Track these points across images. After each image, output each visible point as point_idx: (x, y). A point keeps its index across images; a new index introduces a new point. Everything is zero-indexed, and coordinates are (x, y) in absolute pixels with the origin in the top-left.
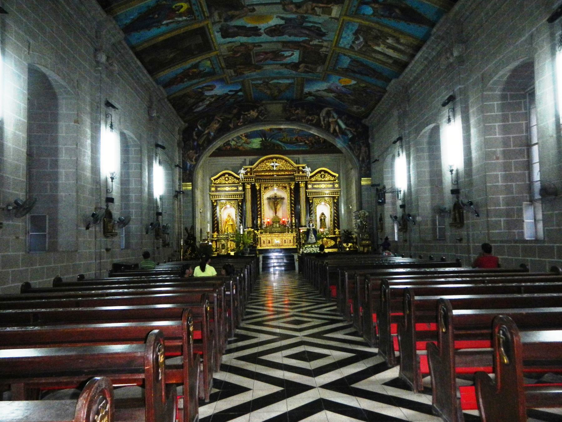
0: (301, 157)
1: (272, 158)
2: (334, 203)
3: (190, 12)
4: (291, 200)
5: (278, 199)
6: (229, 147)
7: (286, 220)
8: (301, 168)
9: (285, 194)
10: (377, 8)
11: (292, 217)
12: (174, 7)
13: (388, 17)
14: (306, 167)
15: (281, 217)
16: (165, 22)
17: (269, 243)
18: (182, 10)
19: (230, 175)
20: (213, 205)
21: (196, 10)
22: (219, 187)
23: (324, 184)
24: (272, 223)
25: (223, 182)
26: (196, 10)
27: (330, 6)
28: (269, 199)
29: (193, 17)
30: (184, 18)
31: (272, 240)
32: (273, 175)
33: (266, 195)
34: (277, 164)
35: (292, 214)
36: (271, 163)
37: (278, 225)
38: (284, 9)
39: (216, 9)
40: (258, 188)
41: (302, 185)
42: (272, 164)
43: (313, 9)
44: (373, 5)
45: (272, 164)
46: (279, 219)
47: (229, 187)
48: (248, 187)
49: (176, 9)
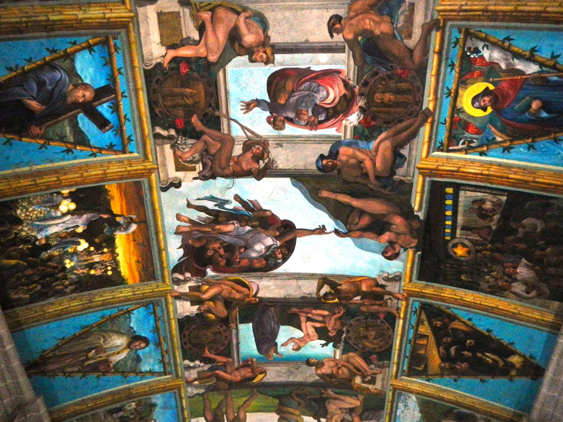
3: (468, 69)
10: (76, 86)
12: (489, 110)
13: (40, 68)
16: (532, 69)
18: (478, 87)
21: (452, 65)
26: (452, 65)
27: (172, 54)
29: (469, 44)
30: (486, 54)
38: (264, 23)
39: (411, 51)
43: (201, 29)
44: (89, 94)
49: (487, 99)
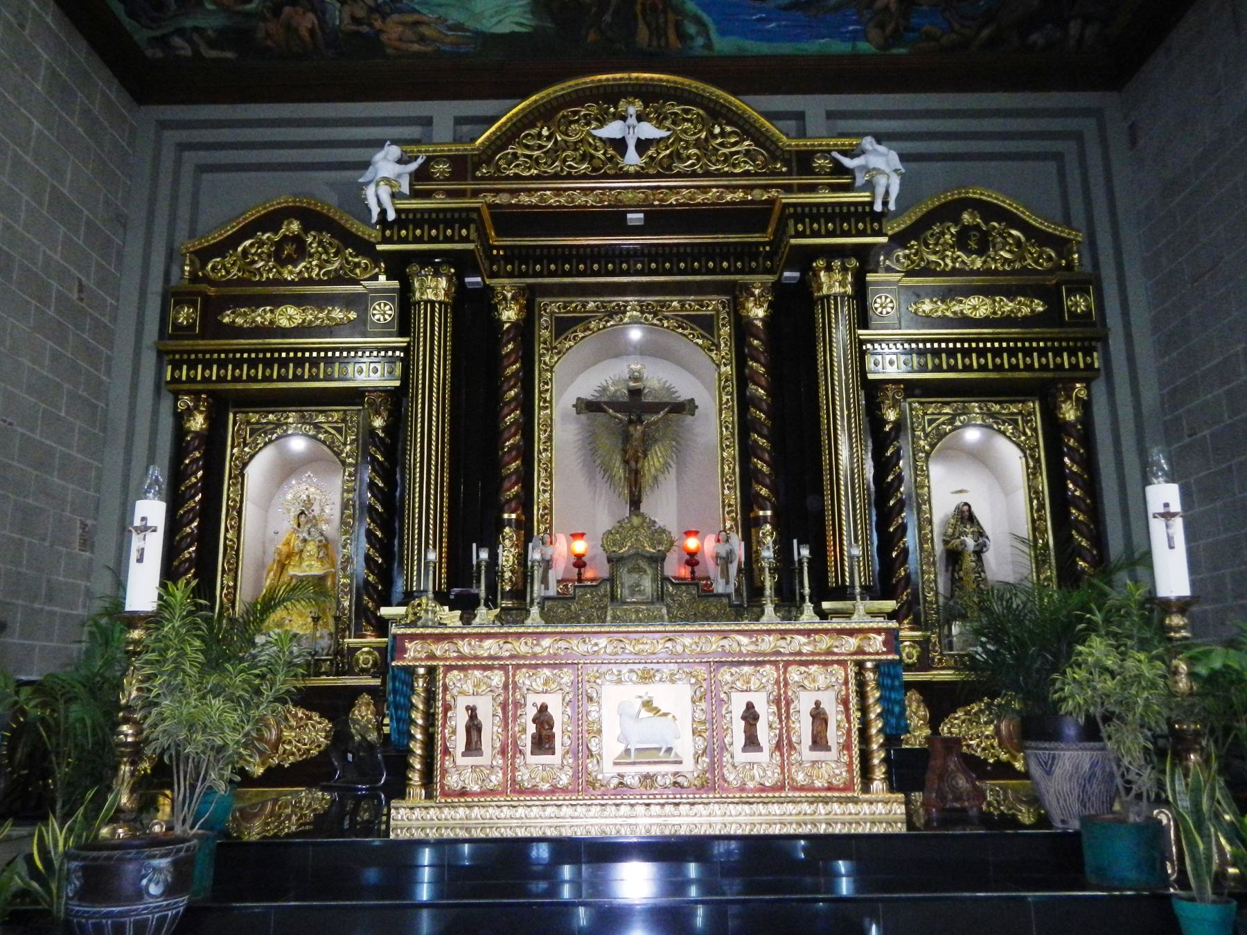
0: (814, 105)
1: (610, 97)
2: (1054, 428)
4: (744, 403)
5: (655, 408)
6: (309, 20)
7: (709, 546)
8: (820, 162)
9: (695, 378)
11: (749, 526)
14: (868, 143)
15: (675, 535)
17: (543, 742)
19: (313, 220)
20: (180, 431)
22: (237, 302)
23: (987, 291)
24: (604, 571)
25: (264, 268)
28: (588, 407)
31: (581, 698)
32: (612, 220)
33: (574, 379)
34: (648, 130)
35: (749, 501)
36: (602, 123)
37: (647, 584)
40: (509, 314)
41: (833, 283)
42: (613, 130)
45: (613, 130)
46: (659, 534)
47: (300, 301)
48: (434, 288)
